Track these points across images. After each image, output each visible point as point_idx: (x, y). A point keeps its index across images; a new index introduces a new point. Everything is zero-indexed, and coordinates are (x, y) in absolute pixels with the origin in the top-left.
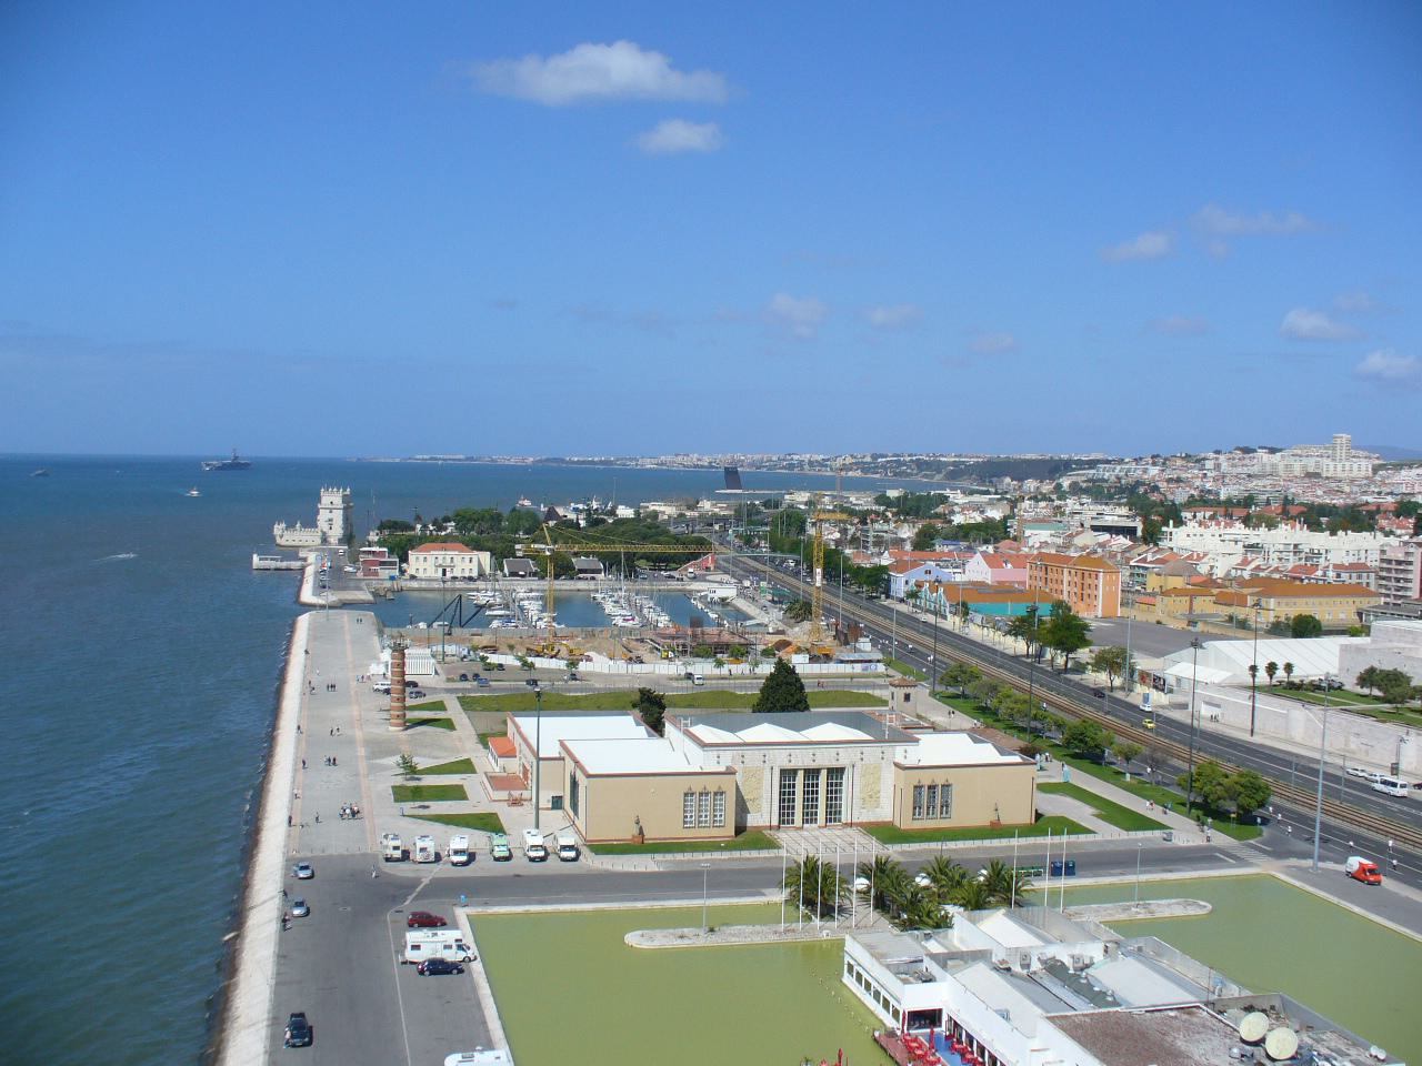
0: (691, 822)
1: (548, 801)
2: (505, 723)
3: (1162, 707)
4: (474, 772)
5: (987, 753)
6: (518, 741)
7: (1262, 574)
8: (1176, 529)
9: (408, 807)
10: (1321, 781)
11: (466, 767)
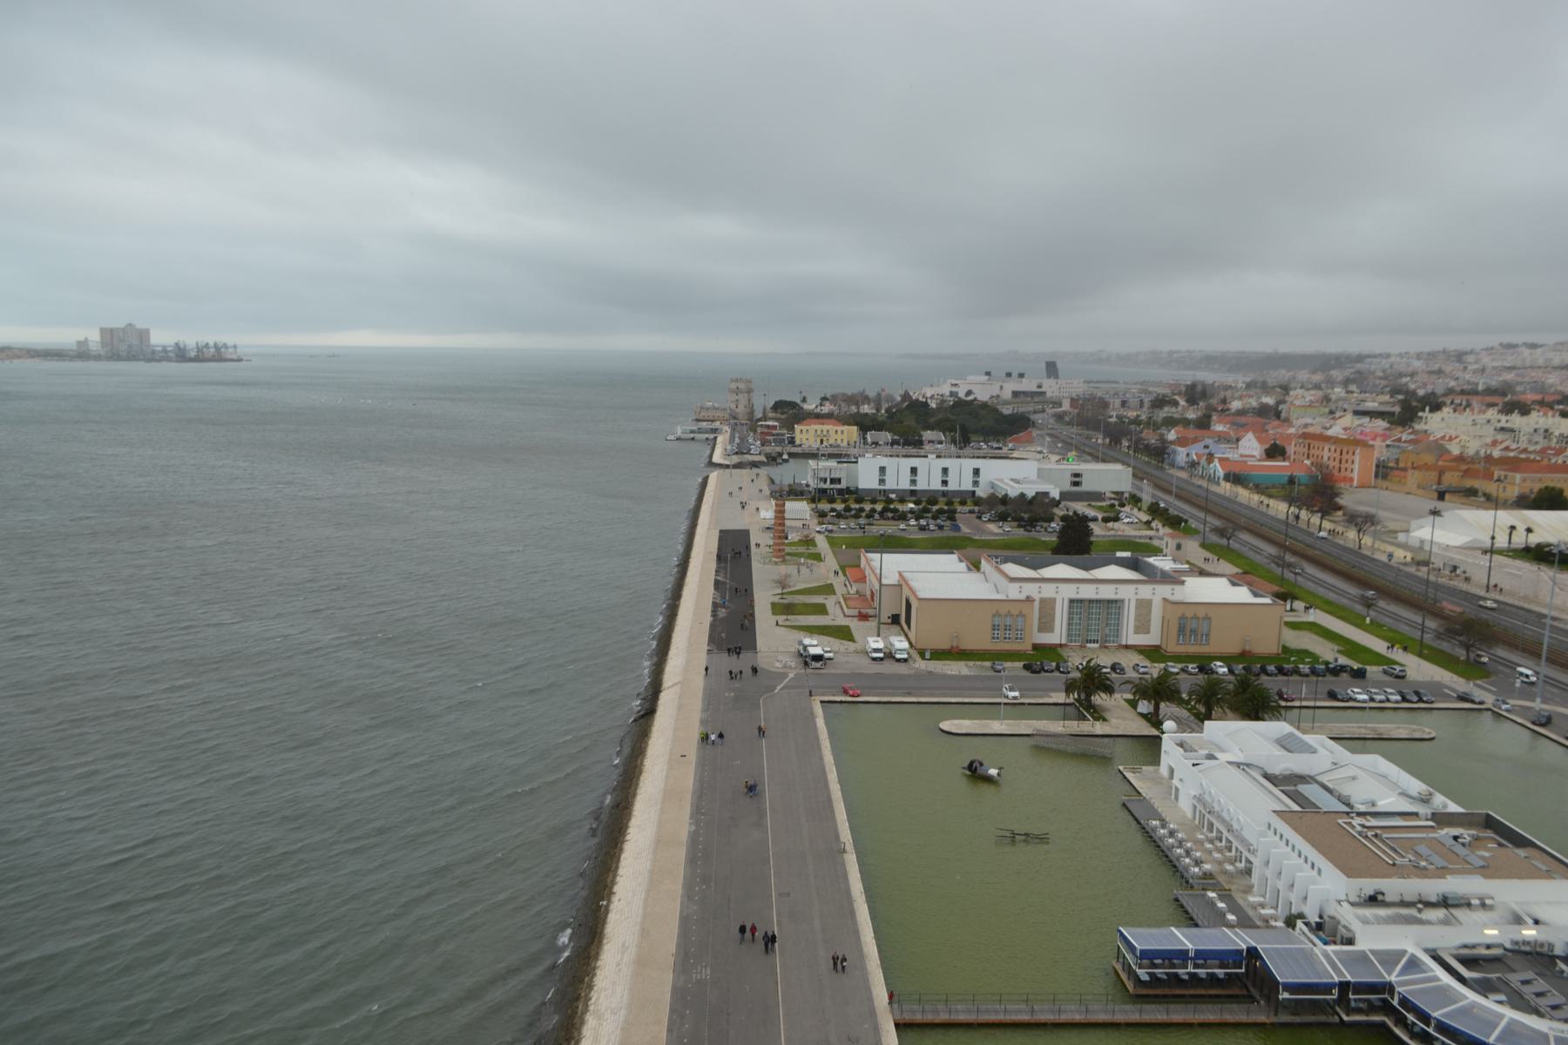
0: (1009, 638)
1: (889, 618)
2: (859, 557)
3: (1405, 564)
4: (835, 594)
5: (1242, 595)
6: (868, 572)
7: (1512, 454)
8: (1430, 415)
9: (781, 618)
10: (1547, 633)
11: (828, 589)
